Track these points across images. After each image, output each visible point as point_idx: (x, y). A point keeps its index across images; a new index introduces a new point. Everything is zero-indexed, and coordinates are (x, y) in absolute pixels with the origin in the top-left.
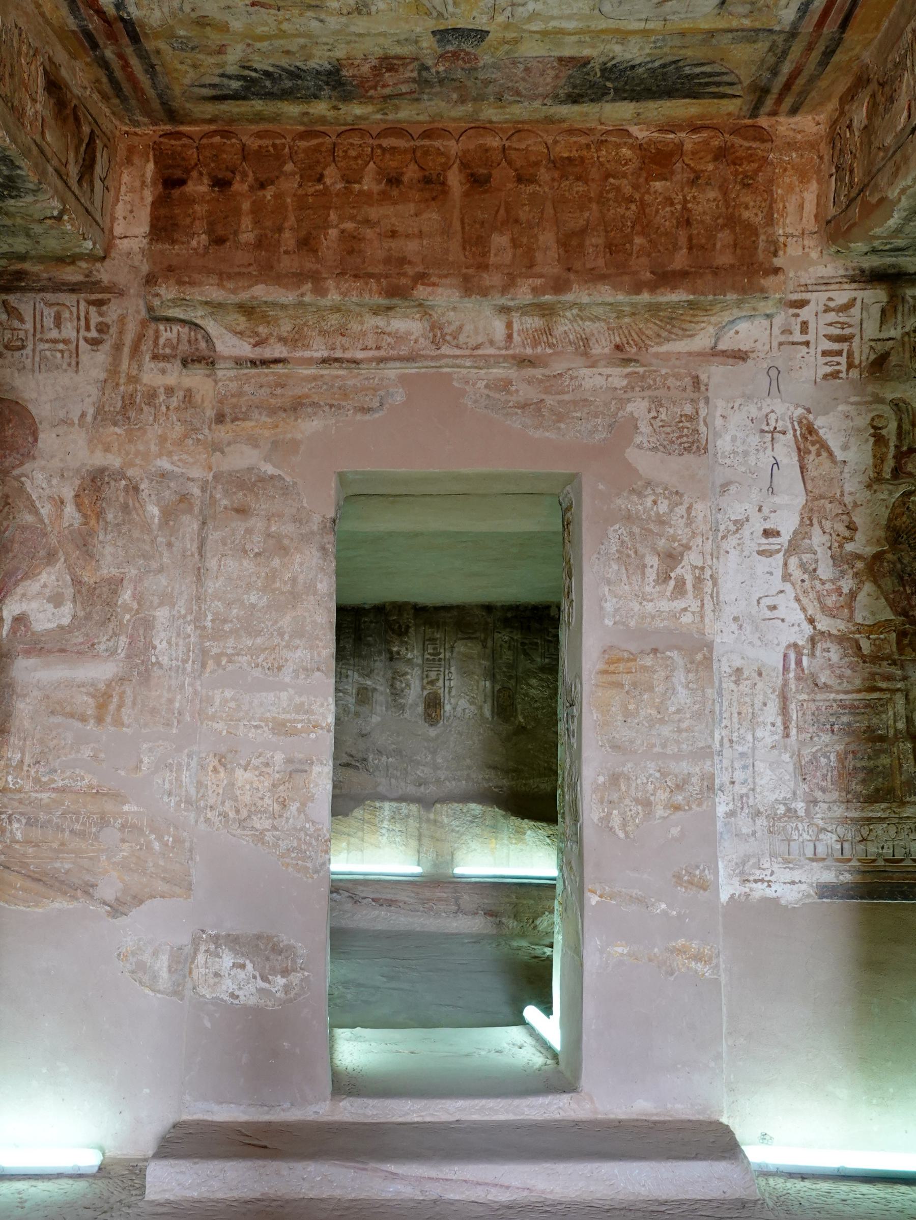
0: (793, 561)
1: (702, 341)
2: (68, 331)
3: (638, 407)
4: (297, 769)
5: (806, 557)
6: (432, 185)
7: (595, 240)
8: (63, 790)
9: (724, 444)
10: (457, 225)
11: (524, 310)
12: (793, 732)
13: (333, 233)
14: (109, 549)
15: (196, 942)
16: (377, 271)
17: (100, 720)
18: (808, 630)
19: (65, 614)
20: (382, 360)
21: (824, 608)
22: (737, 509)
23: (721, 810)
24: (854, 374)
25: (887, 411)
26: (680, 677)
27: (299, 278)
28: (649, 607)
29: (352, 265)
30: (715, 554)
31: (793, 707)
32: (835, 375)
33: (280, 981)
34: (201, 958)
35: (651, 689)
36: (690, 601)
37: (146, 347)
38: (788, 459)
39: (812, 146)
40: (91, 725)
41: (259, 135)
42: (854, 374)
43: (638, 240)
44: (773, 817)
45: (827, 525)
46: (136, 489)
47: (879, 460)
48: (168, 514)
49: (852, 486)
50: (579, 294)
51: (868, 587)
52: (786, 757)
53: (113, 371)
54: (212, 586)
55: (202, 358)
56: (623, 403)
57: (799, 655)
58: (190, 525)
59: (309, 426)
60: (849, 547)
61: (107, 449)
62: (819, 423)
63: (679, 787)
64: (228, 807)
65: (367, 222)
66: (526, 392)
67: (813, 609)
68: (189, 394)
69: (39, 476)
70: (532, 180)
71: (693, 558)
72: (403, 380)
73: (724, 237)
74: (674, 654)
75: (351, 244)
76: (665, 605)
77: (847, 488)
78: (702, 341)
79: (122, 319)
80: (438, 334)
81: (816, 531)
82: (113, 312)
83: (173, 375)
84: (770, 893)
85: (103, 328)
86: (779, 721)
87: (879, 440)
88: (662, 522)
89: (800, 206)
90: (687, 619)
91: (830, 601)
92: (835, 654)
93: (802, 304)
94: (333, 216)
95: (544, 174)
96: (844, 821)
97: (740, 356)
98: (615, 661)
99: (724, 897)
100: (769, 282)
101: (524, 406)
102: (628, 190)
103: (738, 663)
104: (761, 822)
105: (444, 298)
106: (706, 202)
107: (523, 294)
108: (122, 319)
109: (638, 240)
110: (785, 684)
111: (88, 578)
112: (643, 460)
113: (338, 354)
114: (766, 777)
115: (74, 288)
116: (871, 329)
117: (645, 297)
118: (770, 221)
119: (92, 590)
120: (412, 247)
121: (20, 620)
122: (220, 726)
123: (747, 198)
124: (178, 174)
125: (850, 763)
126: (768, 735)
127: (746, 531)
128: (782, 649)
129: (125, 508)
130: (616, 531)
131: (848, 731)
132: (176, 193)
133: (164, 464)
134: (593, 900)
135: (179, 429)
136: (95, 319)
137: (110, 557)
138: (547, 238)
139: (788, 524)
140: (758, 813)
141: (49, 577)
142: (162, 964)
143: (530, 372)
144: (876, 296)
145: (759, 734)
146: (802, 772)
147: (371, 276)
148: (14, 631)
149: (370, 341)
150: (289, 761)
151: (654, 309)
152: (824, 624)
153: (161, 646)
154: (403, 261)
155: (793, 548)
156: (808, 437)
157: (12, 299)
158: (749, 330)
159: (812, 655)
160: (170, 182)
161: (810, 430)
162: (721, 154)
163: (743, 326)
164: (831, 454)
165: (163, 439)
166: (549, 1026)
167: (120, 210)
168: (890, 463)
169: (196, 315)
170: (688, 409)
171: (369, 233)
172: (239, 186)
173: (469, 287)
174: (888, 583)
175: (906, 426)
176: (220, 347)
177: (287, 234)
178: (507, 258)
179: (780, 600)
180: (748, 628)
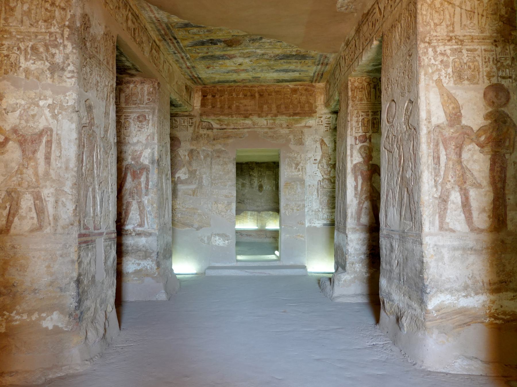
0: (320, 165)
1: (303, 124)
2: (186, 124)
3: (291, 137)
4: (229, 204)
6: (253, 96)
7: (283, 106)
8: (187, 208)
9: (307, 143)
10: (257, 104)
11: (270, 120)
13: (234, 105)
14: (194, 164)
15: (212, 235)
16: (242, 113)
17: (193, 195)
18: (322, 178)
19: (187, 176)
20: (244, 128)
21: (325, 174)
22: (310, 155)
23: (306, 210)
26: (299, 186)
27: (228, 115)
28: (293, 174)
29: (238, 112)
30: (306, 164)
31: (319, 192)
32: (327, 130)
33: (227, 242)
34: (213, 238)
35: (293, 188)
36: (300, 173)
37: (200, 126)
38: (319, 146)
39: (323, 88)
40: (192, 196)
41: (220, 87)
42: (331, 130)
43: (291, 106)
44: (315, 212)
46: (199, 153)
48: (205, 157)
50: (279, 117)
53: (194, 131)
54: (213, 171)
55: (210, 128)
56: (288, 136)
58: (209, 159)
59: (231, 141)
60: (330, 162)
61: (193, 145)
63: (299, 206)
64: (217, 211)
65: (241, 103)
66: (270, 134)
67: (323, 174)
68: (208, 135)
69: (181, 151)
70: (271, 95)
71: (301, 165)
72: (248, 132)
73: (307, 105)
74: (298, 182)
75: (238, 108)
76: (296, 173)
78: (303, 124)
79: (196, 122)
80: (254, 124)
81: (324, 159)
82: (194, 120)
83: (205, 131)
84: (315, 225)
85: (192, 123)
88: (295, 158)
89: (321, 99)
90: (300, 176)
91: (326, 172)
93: (321, 117)
94: (234, 102)
95: (273, 94)
96: (328, 212)
97: (310, 127)
98: (286, 184)
99: (307, 226)
100: (314, 115)
101: (270, 137)
102: (289, 96)
103: (309, 184)
104: (313, 213)
105: (255, 118)
106: (303, 99)
107: (269, 117)
108: (196, 122)
109: (291, 106)
111: (191, 169)
112: (292, 146)
113: (236, 127)
114: (314, 204)
115: (187, 116)
117: (291, 118)
118: (315, 102)
119: (191, 172)
120: (249, 108)
121: (179, 177)
122: (215, 196)
123: (311, 98)
124: (206, 95)
125: (329, 202)
126: (315, 197)
127: (311, 159)
129: (197, 157)
130: (287, 160)
131: (329, 196)
132: (205, 98)
133: (204, 148)
134: (283, 227)
135: (206, 141)
136: (191, 121)
137: (195, 166)
138: (274, 106)
139: (319, 158)
141: (184, 170)
142: (206, 239)
143: (271, 130)
146: (321, 204)
147: (241, 114)
148: (177, 179)
149: (242, 125)
150: (228, 202)
151: (293, 119)
152: (325, 176)
153: (204, 182)
154: (247, 110)
155: (320, 162)
156: (322, 142)
157: (175, 118)
158: (311, 122)
160: (204, 96)
161: (323, 141)
162: (306, 90)
163: (310, 121)
165: (203, 143)
166: (277, 253)
167: (195, 101)
169: (210, 121)
170: (300, 137)
171: (241, 105)
172: (217, 96)
173: (260, 116)
176: (214, 126)
177: (226, 105)
178: (267, 109)
179: (317, 172)
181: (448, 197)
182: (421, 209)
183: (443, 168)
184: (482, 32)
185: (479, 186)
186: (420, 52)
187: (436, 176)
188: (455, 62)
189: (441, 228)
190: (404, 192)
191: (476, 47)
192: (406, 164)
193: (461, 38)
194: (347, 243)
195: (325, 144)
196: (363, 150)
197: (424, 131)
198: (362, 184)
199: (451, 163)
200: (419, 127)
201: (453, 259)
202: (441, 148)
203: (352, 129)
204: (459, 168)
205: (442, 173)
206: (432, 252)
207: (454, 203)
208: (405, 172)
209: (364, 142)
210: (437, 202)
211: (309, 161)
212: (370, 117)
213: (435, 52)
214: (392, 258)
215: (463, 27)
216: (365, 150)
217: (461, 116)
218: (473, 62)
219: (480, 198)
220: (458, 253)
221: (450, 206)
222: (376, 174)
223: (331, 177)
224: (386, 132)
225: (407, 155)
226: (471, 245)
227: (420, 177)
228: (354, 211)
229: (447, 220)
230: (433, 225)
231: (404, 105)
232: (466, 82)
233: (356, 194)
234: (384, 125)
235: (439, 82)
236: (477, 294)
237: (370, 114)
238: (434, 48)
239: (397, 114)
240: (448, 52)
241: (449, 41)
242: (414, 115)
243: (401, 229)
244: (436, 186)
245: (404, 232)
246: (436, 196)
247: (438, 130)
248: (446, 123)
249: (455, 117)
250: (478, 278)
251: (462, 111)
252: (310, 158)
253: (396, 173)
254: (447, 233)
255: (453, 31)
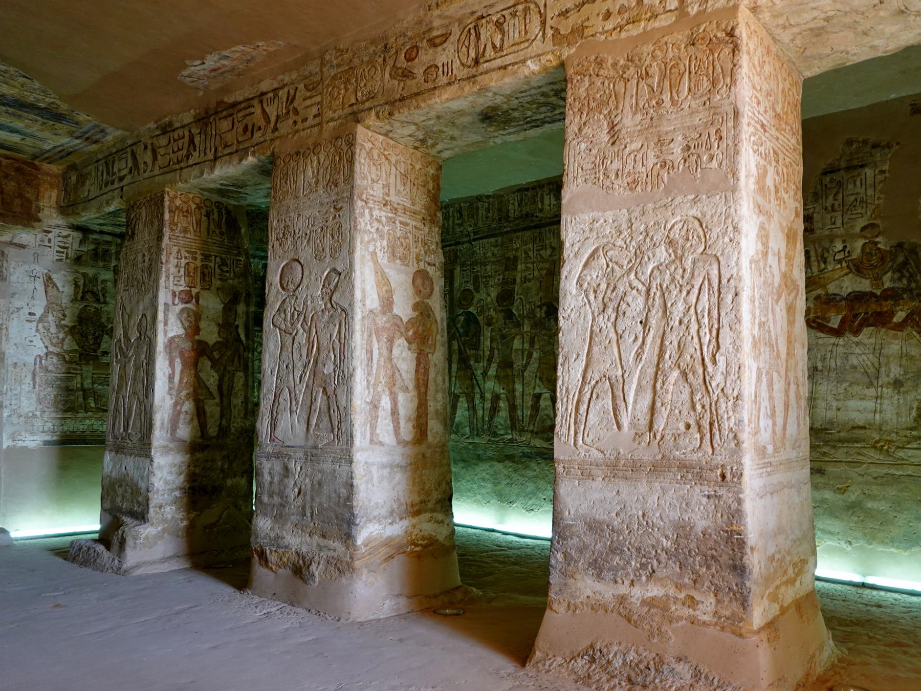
0: (40, 325)
5: (45, 324)
12: (37, 387)
18: (45, 351)
21: (52, 344)
23: (5, 414)
24: (68, 261)
25: (80, 276)
42: (68, 261)
44: (27, 417)
45: (55, 313)
47: (76, 293)
49: (65, 301)
51: (69, 337)
52: (34, 396)
57: (41, 359)
60: (63, 322)
62: (54, 277)
77: (64, 301)
86: (31, 383)
87: (76, 286)
91: (54, 341)
92: (55, 360)
99: (5, 446)
104: (22, 419)
110: (35, 369)
114: (25, 403)
116: (76, 246)
128: (34, 357)
139: (39, 311)
140: (21, 416)
144: (78, 235)
145: (23, 387)
146: (40, 401)
155: (41, 320)
159: (46, 359)
164: (58, 288)
168: (80, 294)
174: (77, 336)
175: (87, 283)
180: (20, 348)
181: (379, 401)
182: (352, 417)
183: (375, 366)
184: (413, 204)
185: (406, 390)
186: (357, 211)
187: (369, 374)
188: (390, 234)
189: (372, 441)
190: (317, 393)
191: (409, 221)
192: (323, 354)
193: (395, 206)
194: (152, 472)
195: (55, 285)
196: (185, 315)
197: (358, 316)
198: (182, 372)
199: (382, 359)
200: (352, 309)
201: (382, 479)
202: (374, 339)
203: (168, 277)
204: (389, 367)
205: (374, 371)
206: (363, 473)
207: (384, 410)
208: (320, 365)
209: (186, 303)
210: (368, 408)
211: (15, 315)
212: (199, 263)
213: (371, 215)
214: (285, 487)
215: (398, 192)
216: (188, 316)
217: (392, 303)
218: (406, 238)
219: (406, 403)
220: (386, 472)
221: (381, 413)
222: (205, 357)
223: (65, 351)
224: (279, 303)
225: (324, 342)
226: (397, 462)
227: (352, 375)
228: (166, 416)
229: (378, 431)
230: (365, 438)
231: (323, 273)
232: (398, 261)
233: (170, 389)
234: (273, 291)
235: (374, 254)
236: (401, 519)
237: (199, 257)
238: (371, 209)
239: (305, 281)
240: (384, 219)
241: (385, 205)
242: (344, 292)
243: (310, 443)
244: (368, 388)
245: (316, 447)
246: (368, 400)
247: (372, 316)
248: (379, 308)
249: (387, 303)
250: (402, 501)
251: (394, 297)
252: (18, 309)
253: (299, 365)
254: (377, 446)
255: (388, 195)
